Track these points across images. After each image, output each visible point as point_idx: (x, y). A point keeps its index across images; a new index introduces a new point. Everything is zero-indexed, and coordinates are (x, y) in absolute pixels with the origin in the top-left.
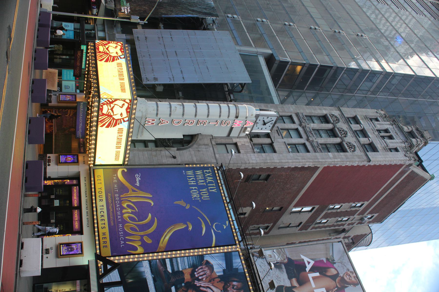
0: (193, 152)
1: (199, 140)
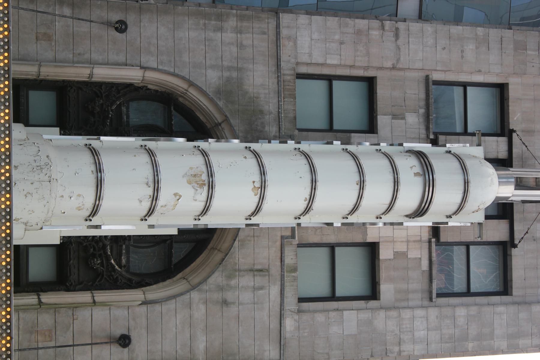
0: (199, 311)
1: (241, 256)
